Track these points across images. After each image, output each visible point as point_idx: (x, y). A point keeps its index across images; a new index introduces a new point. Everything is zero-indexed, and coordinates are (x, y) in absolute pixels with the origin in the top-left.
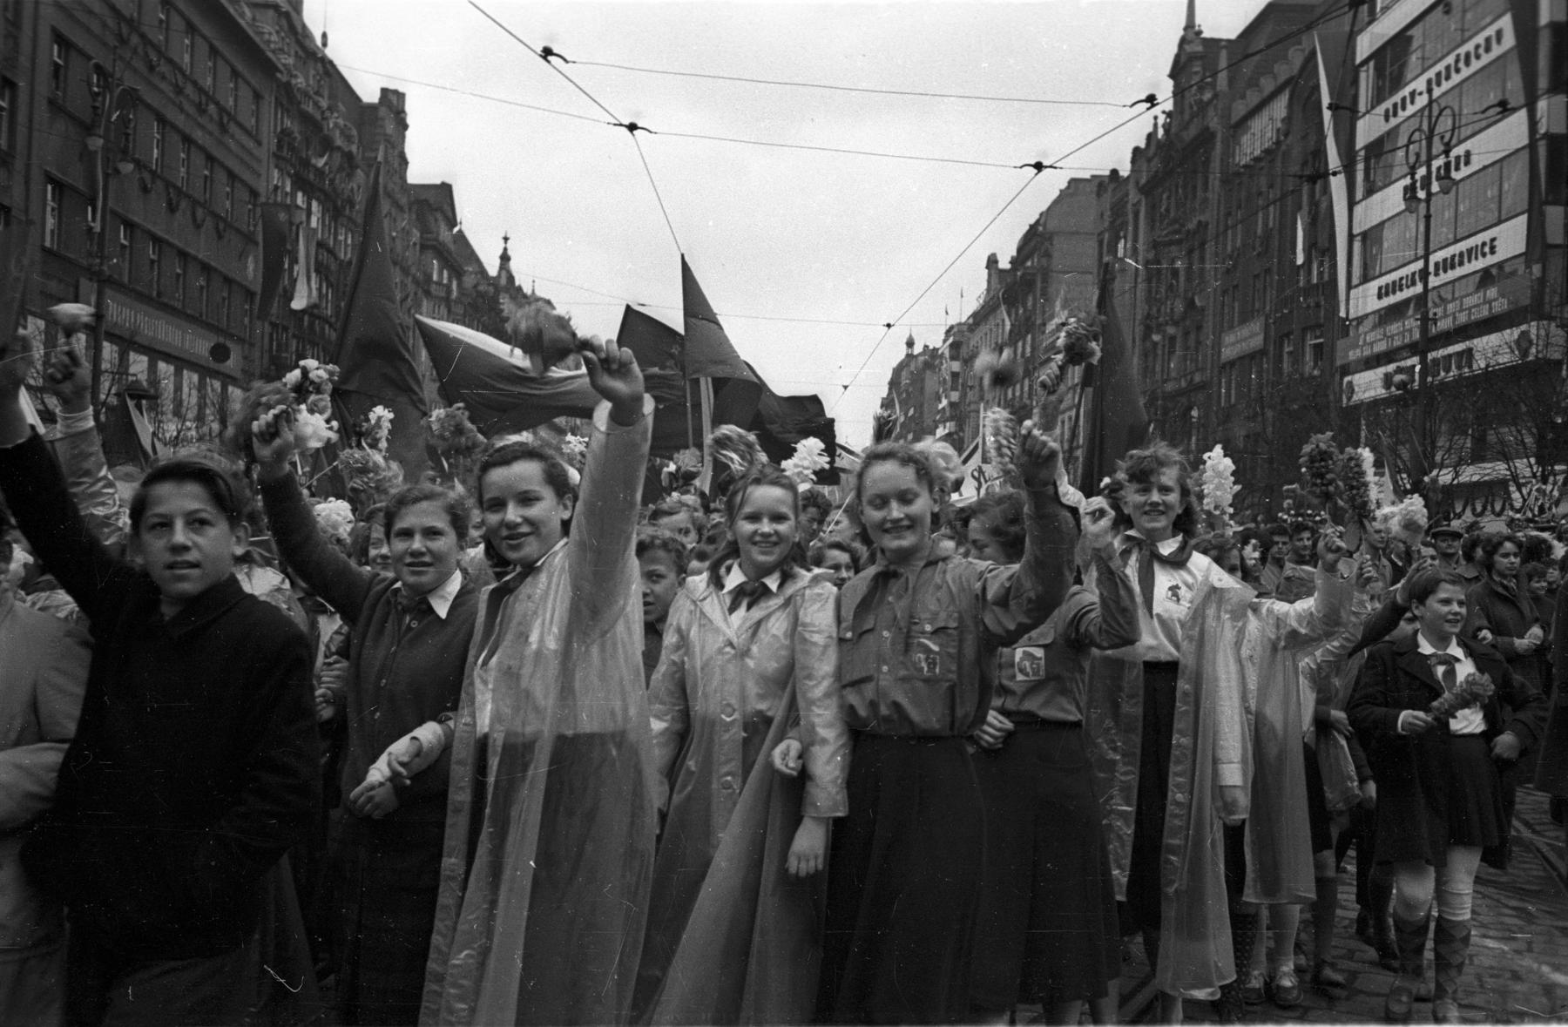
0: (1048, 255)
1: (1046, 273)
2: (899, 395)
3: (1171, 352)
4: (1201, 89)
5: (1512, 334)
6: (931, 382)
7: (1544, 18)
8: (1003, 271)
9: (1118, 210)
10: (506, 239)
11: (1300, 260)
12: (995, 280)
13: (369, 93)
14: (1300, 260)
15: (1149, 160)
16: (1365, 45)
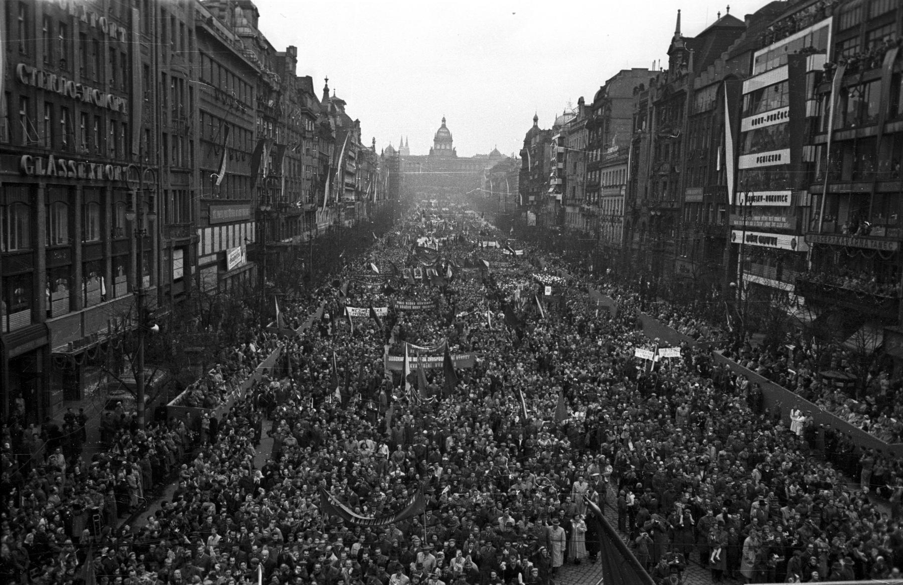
0: (609, 109)
1: (608, 119)
2: (530, 152)
3: (664, 188)
4: (682, 66)
5: (790, 238)
6: (548, 148)
7: (808, 114)
8: (587, 107)
9: (643, 105)
10: (326, 80)
11: (718, 169)
12: (582, 111)
13: (280, 47)
14: (718, 169)
15: (658, 90)
16: (748, 87)
